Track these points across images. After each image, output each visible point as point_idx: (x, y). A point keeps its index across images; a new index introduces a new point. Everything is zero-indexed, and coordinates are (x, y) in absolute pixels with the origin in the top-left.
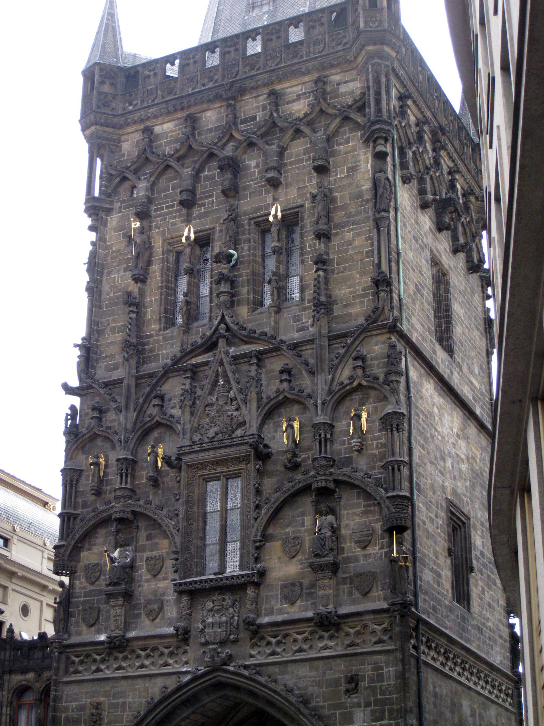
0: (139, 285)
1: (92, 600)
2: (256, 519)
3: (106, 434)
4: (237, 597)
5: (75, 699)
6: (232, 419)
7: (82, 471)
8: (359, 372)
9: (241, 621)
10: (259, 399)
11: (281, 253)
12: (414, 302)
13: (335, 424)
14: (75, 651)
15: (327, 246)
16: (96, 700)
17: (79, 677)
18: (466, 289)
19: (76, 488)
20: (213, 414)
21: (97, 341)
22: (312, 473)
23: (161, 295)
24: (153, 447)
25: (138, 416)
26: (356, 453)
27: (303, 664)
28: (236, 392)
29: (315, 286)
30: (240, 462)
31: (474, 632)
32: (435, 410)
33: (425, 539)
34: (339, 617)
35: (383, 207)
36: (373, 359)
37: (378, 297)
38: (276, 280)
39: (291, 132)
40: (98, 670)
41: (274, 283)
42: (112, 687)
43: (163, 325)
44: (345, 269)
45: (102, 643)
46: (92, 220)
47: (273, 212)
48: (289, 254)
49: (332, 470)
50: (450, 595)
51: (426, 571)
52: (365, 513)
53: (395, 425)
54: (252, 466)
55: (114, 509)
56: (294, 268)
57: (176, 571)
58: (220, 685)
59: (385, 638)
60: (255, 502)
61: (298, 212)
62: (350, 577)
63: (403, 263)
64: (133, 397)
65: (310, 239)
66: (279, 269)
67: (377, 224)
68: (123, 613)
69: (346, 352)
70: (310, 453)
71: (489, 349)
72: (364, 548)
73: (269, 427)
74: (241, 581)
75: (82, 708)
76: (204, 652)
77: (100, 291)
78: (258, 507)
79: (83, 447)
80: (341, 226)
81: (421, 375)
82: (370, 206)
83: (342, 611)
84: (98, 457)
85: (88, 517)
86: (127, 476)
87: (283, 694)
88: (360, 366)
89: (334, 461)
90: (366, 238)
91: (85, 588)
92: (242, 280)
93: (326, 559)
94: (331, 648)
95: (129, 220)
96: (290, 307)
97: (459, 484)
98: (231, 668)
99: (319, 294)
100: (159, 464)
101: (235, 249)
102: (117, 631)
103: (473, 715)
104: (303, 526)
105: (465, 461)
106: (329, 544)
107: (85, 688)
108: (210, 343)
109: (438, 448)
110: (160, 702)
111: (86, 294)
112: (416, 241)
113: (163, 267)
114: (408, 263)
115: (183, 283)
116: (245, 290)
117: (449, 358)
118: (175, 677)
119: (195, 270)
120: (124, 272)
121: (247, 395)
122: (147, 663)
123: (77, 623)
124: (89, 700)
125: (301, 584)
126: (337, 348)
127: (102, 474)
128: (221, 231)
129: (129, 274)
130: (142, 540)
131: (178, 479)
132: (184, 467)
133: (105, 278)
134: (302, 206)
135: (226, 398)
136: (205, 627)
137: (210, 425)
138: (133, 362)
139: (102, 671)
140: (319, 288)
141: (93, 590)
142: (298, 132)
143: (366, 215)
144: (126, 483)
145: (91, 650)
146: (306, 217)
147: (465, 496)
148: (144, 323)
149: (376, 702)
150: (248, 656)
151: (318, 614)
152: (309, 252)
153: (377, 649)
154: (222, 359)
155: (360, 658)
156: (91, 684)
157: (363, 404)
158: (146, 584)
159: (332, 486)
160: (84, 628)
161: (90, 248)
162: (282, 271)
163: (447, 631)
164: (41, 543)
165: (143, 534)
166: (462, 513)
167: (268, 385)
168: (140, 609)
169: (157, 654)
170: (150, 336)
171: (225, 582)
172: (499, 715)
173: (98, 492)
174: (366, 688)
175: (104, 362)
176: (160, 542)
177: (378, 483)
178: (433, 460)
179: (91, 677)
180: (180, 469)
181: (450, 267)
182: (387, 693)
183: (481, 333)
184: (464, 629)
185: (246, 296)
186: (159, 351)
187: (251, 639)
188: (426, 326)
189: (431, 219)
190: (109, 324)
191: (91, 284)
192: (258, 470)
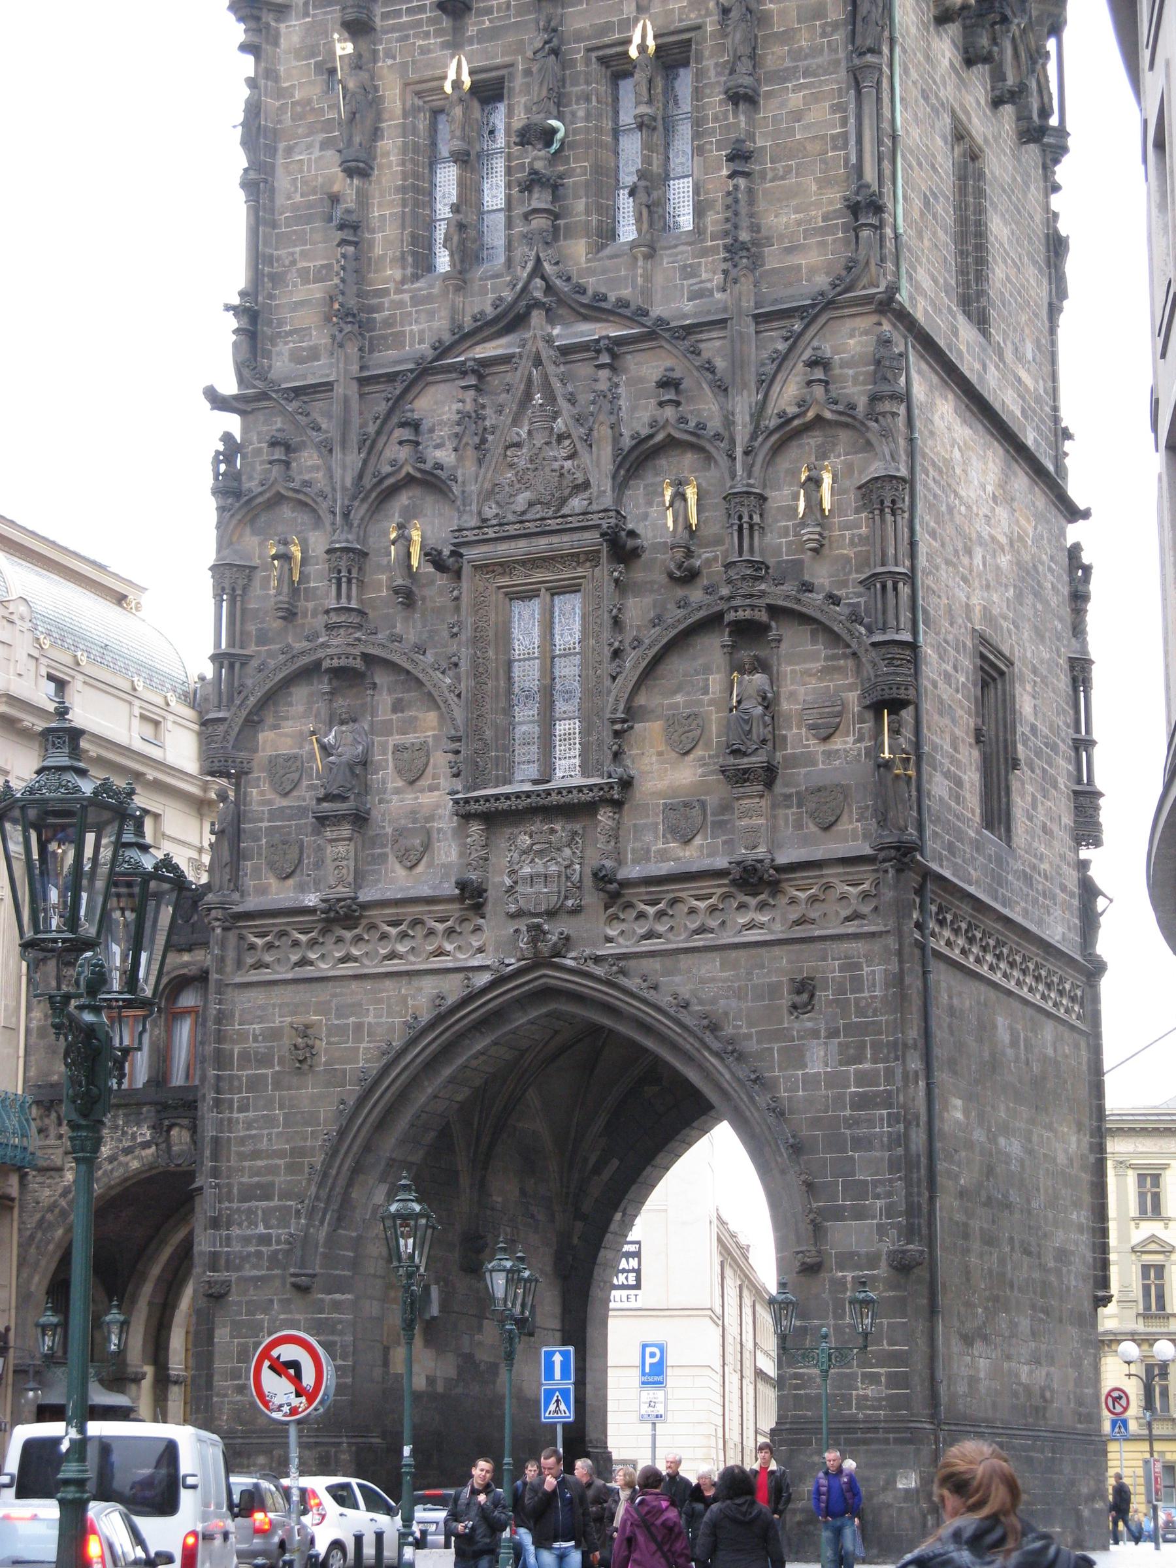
0: (356, 181)
2: (614, 678)
3: (301, 497)
4: (577, 827)
6: (562, 475)
7: (253, 568)
8: (819, 390)
9: (588, 871)
10: (617, 437)
11: (654, 129)
12: (920, 236)
13: (768, 493)
15: (751, 121)
16: (299, 1019)
17: (266, 975)
18: (1014, 179)
19: (242, 602)
20: (522, 463)
21: (271, 297)
22: (725, 591)
23: (404, 206)
24: (401, 527)
25: (365, 462)
26: (809, 553)
27: (710, 955)
28: (570, 422)
29: (728, 207)
30: (578, 563)
31: (1018, 884)
32: (957, 454)
33: (936, 717)
34: (780, 869)
35: (869, 42)
36: (844, 364)
37: (857, 237)
38: (646, 188)
40: (304, 962)
41: (642, 196)
42: (334, 996)
43: (409, 271)
44: (788, 169)
45: (311, 911)
46: (246, 31)
47: (637, 39)
48: (669, 128)
49: (763, 587)
50: (978, 819)
51: (938, 778)
52: (826, 671)
53: (887, 503)
54: (604, 573)
55: (330, 651)
56: (678, 161)
57: (457, 775)
58: (547, 993)
59: (866, 909)
60: (611, 645)
61: (689, 40)
62: (798, 793)
63: (903, 157)
64: (356, 421)
65: (715, 101)
66: (650, 164)
67: (856, 79)
68: (352, 854)
69: (791, 349)
70: (719, 551)
71: (1055, 301)
72: (826, 739)
73: (636, 493)
74: (587, 797)
75: (274, 1034)
76: (517, 931)
77: (272, 190)
78: (617, 654)
79: (253, 521)
80: (782, 76)
81: (931, 386)
82: (839, 37)
83: (784, 858)
84: (286, 543)
85: (272, 663)
86: (349, 581)
87: (672, 1011)
88: (820, 380)
89: (767, 568)
90: (832, 106)
91: (269, 802)
92: (575, 183)
93: (753, 759)
94: (761, 926)
95: (326, 34)
96: (676, 246)
97: (995, 598)
98: (569, 963)
99: (736, 227)
100: (415, 562)
101: (559, 117)
102: (340, 889)
103: (1014, 1043)
104: (706, 692)
105: (1007, 548)
106: (759, 731)
108: (511, 316)
109: (959, 530)
110: (432, 1025)
111: (241, 195)
112: (926, 98)
113: (405, 144)
114: (912, 152)
115: (448, 179)
116: (580, 205)
117: (981, 339)
118: (461, 976)
119: (473, 153)
120: (321, 149)
121: (591, 430)
122: (401, 948)
123: (257, 870)
124: (289, 1019)
125: (703, 804)
126: (772, 339)
127: (296, 578)
128: (528, 72)
129: (332, 157)
130: (384, 713)
131: (456, 593)
132: (467, 570)
133: (280, 160)
134: (698, 28)
135: (547, 433)
136: (516, 883)
137: (517, 486)
138: (352, 349)
139: (311, 963)
140: (736, 214)
143: (834, 57)
144: (349, 598)
145: (288, 924)
146: (707, 53)
147: (1005, 618)
148: (369, 265)
150: (602, 939)
151: (738, 863)
152: (713, 132)
153: (850, 930)
154: (538, 353)
155: (819, 946)
156: (291, 988)
157: (823, 456)
158: (395, 798)
159: (763, 617)
160: (273, 881)
161: (246, 92)
162: (656, 168)
163: (971, 889)
164: (126, 686)
165: (384, 700)
166: (1000, 654)
167: (633, 409)
168: (384, 846)
169: (419, 932)
170: (384, 293)
171: (554, 799)
172: (1058, 1039)
173: (290, 615)
174: (829, 1003)
175: (286, 343)
176: (421, 715)
177: (855, 617)
178: (951, 557)
179: (290, 976)
180: (458, 574)
181: (986, 140)
182: (870, 1013)
183: (1040, 271)
184: (1001, 881)
185: (583, 218)
186: (402, 325)
187: (607, 908)
188: (941, 281)
189: (953, 42)
190: (293, 263)
191: (252, 175)
192: (617, 581)
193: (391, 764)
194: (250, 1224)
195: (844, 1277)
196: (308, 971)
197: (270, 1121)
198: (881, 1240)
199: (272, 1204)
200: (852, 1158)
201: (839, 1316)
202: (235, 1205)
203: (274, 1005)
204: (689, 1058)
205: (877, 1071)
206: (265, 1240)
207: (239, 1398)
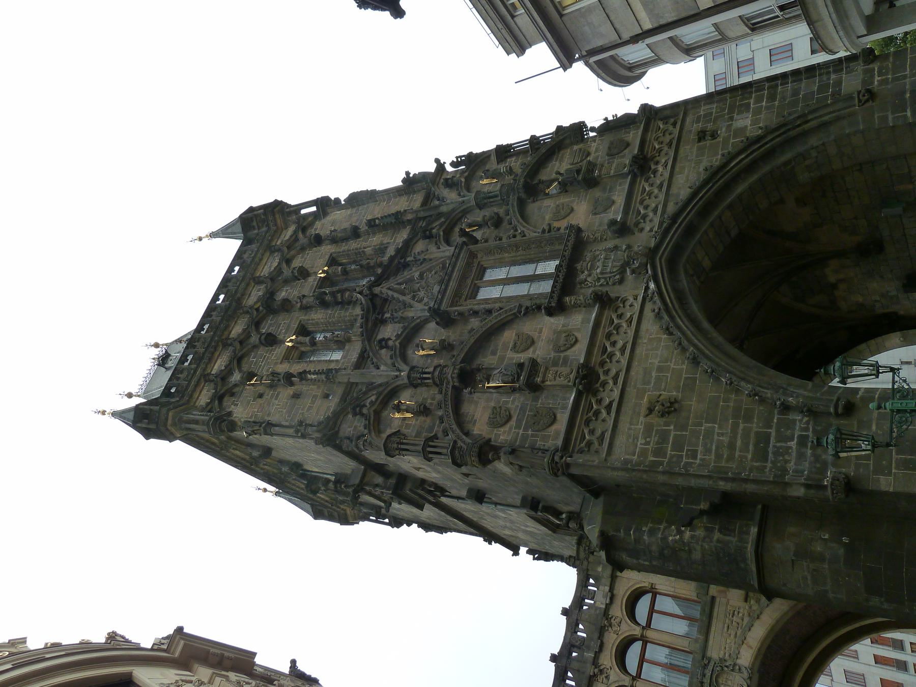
1: (527, 417)
5: (634, 440)
14: (576, 439)
16: (644, 411)
30: (472, 264)
39: (284, 265)
40: (609, 407)
75: (648, 429)
91: (511, 428)
122: (620, 344)
141: (518, 417)
142: (288, 262)
149: (731, 111)
155: (684, 134)
156: (622, 418)
158: (538, 352)
160: (553, 428)
168: (560, 357)
193: (520, 355)
196: (615, 405)
198: (857, 70)
199: (773, 434)
201: (905, 77)
202: (769, 465)
203: (630, 429)
204: (728, 187)
206: (803, 441)
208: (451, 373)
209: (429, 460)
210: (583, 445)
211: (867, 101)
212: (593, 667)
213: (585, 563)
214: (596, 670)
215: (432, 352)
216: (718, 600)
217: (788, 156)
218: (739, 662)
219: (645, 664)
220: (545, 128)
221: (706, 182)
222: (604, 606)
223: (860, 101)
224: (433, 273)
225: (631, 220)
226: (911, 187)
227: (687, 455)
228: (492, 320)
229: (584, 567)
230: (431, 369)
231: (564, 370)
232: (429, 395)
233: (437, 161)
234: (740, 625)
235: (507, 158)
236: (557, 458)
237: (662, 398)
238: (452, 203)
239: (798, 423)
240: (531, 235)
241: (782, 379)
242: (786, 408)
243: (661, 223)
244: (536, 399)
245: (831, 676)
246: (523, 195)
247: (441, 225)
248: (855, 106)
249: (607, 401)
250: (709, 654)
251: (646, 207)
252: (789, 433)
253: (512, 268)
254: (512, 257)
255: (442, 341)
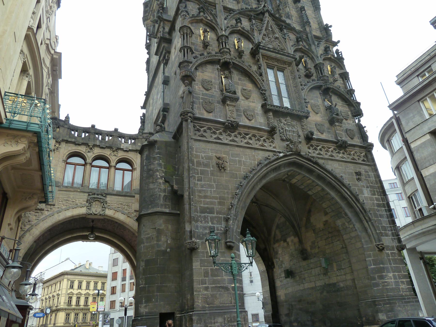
5: (203, 151)
14: (200, 124)
16: (218, 155)
40: (218, 138)
75: (210, 158)
91: (202, 91)
107: (210, 146)
122: (251, 142)
124: (215, 154)
145: (212, 126)
158: (242, 101)
168: (241, 113)
193: (240, 93)
194: (205, 222)
195: (388, 252)
197: (211, 186)
198: (393, 243)
199: (214, 215)
200: (380, 219)
201: (390, 264)
202: (199, 214)
203: (209, 149)
204: (333, 188)
205: (379, 198)
207: (206, 292)
208: (227, 58)
209: (180, 51)
210: (198, 127)
211: (378, 248)
212: (93, 145)
213: (141, 137)
214: (91, 146)
215: (237, 47)
216: (133, 199)
217: (350, 214)
218: (107, 210)
219: (98, 169)
220: (359, 96)
221: (335, 177)
222: (122, 147)
223: (378, 245)
224: (279, 44)
225: (314, 143)
226: (335, 269)
227: (199, 177)
228: (257, 77)
229: (139, 137)
230: (227, 47)
231: (235, 115)
232: (214, 47)
233: (339, 42)
234: (124, 209)
235: (342, 78)
236: (189, 114)
237: (226, 163)
238: (317, 51)
239: (220, 226)
240: (303, 93)
241: (241, 218)
242: (227, 220)
243: (313, 157)
244: (218, 102)
245: (115, 253)
246: (323, 87)
247: (304, 47)
248: (376, 243)
249: (221, 137)
250: (108, 196)
251: (321, 150)
252: (215, 222)
253: (285, 85)
254: (290, 84)
255: (243, 52)
